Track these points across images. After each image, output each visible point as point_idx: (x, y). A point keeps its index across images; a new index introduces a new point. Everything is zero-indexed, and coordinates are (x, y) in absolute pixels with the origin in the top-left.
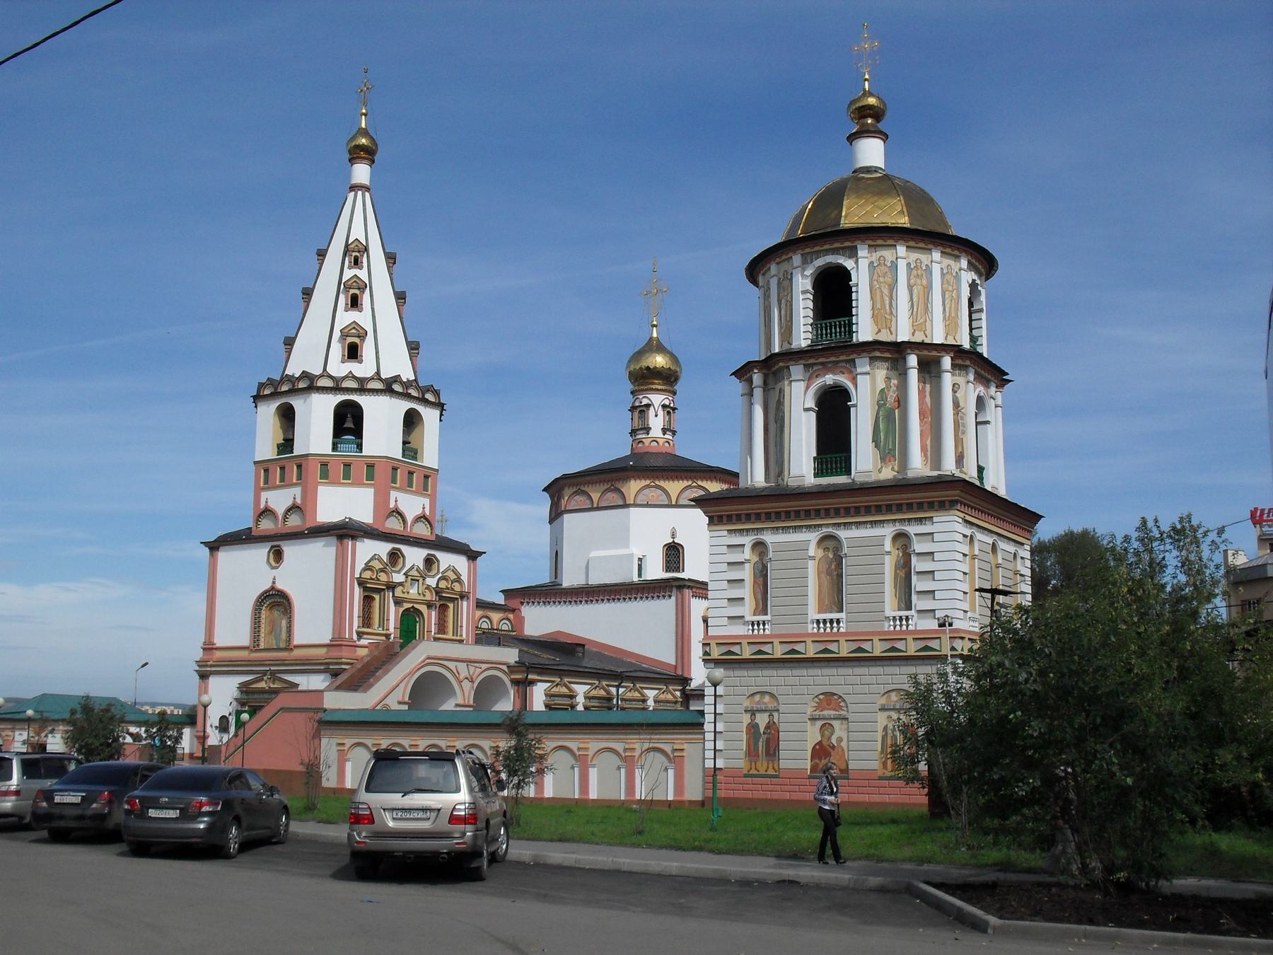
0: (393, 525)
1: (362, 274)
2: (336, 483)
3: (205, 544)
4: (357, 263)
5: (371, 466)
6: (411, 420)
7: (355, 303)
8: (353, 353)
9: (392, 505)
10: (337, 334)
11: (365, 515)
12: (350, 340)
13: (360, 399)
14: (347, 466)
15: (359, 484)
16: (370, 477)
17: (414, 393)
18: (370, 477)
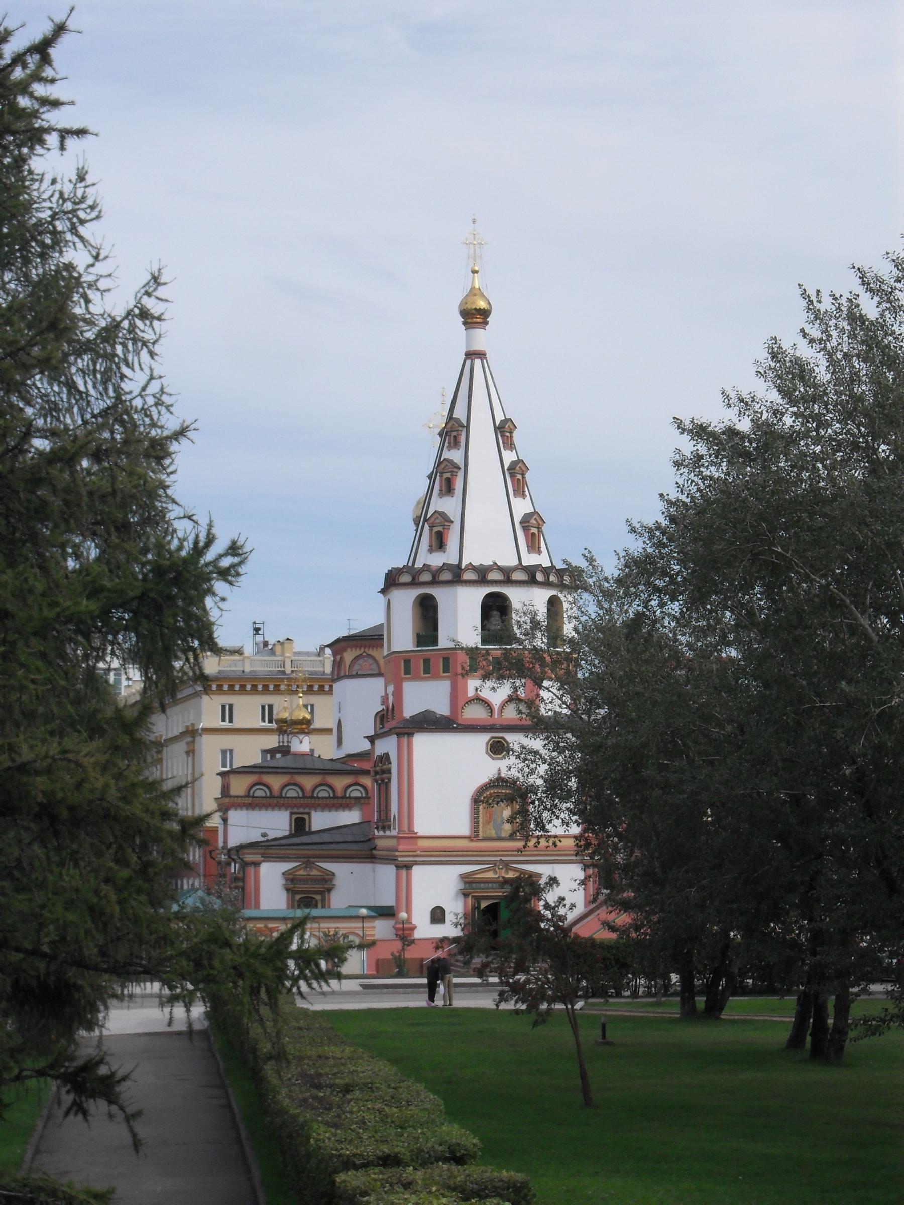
0: (474, 713)
1: (455, 456)
2: (417, 678)
3: (367, 737)
4: (455, 444)
5: (446, 660)
6: (495, 608)
7: (448, 489)
8: (439, 543)
9: (471, 693)
10: (427, 526)
11: (443, 709)
12: (436, 529)
13: (438, 593)
14: (427, 661)
15: (436, 677)
16: (446, 669)
17: (493, 576)
18: (446, 669)
